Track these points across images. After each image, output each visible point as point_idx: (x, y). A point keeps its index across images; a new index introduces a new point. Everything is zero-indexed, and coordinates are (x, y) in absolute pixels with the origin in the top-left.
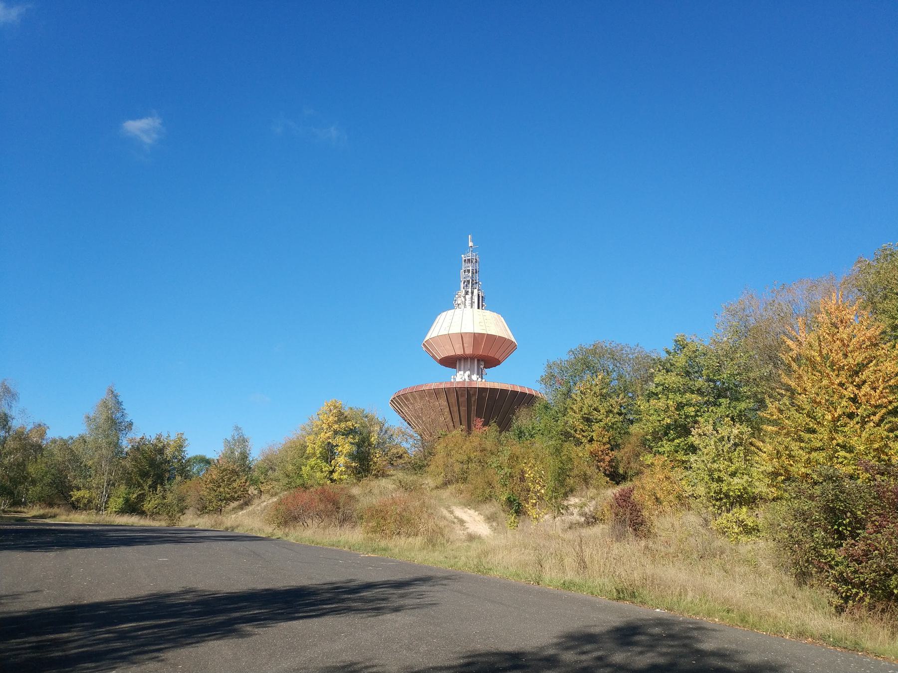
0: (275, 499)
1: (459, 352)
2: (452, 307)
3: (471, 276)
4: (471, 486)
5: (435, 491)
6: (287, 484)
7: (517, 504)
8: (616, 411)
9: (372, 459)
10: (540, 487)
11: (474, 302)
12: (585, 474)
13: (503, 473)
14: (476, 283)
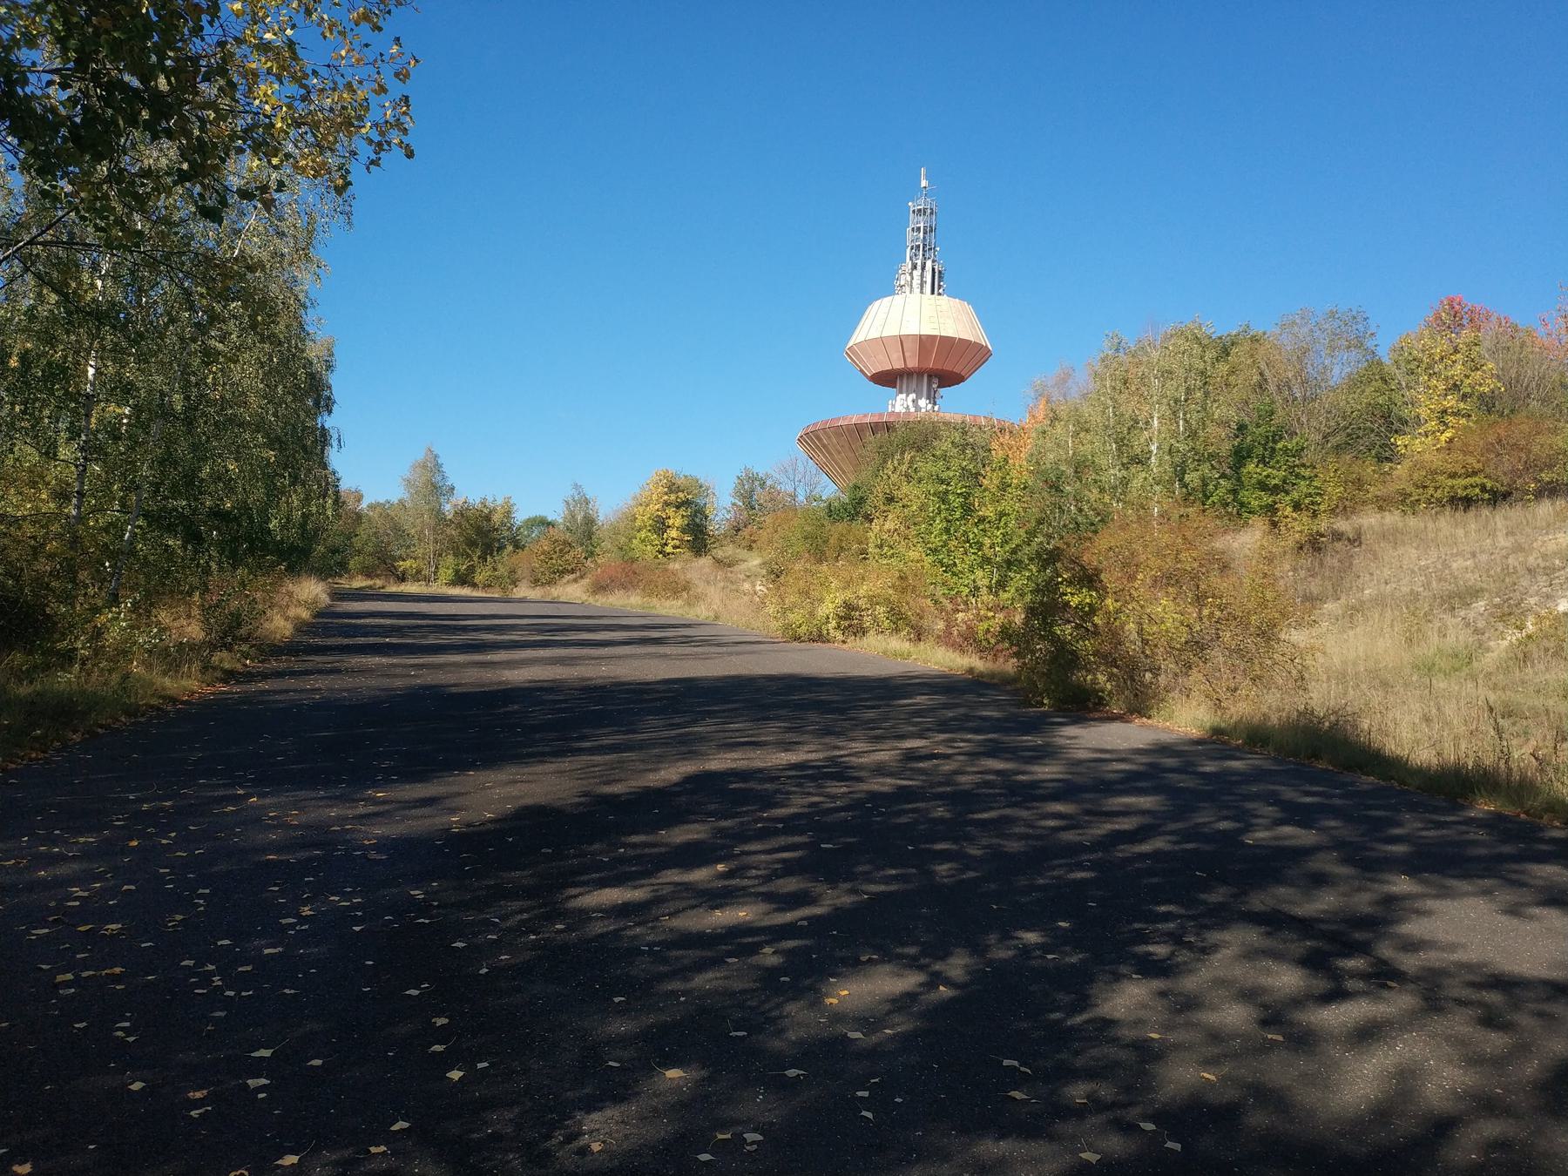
2: (892, 293)
11: (926, 282)
14: (930, 249)
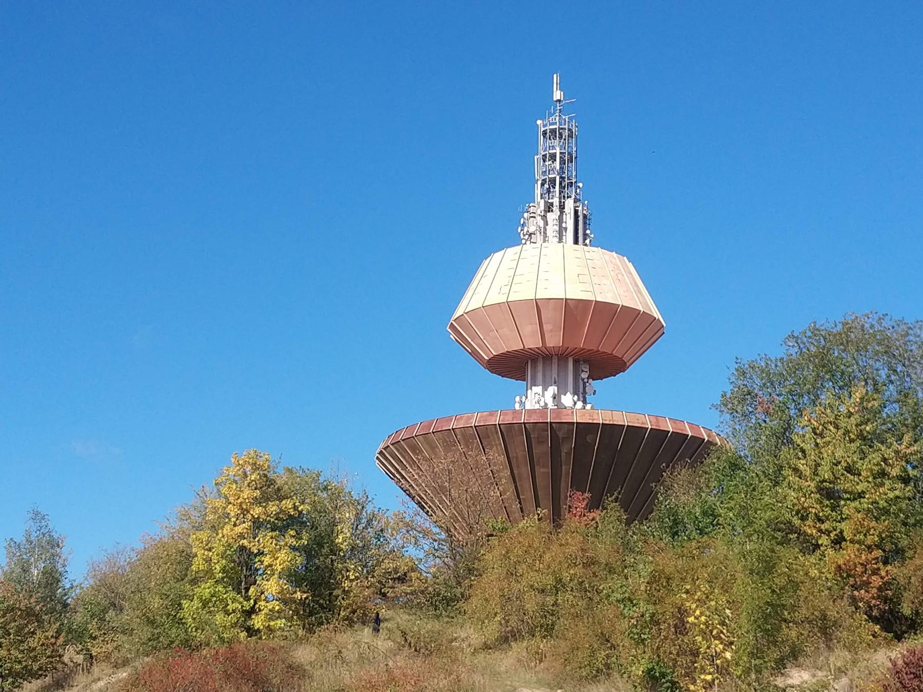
0: (123, 674)
1: (533, 342)
2: (517, 242)
3: (558, 168)
4: (563, 644)
5: (481, 656)
6: (150, 640)
7: (668, 684)
8: (895, 472)
9: (338, 584)
10: (721, 646)
11: (566, 229)
12: (824, 617)
13: (636, 615)
14: (571, 184)
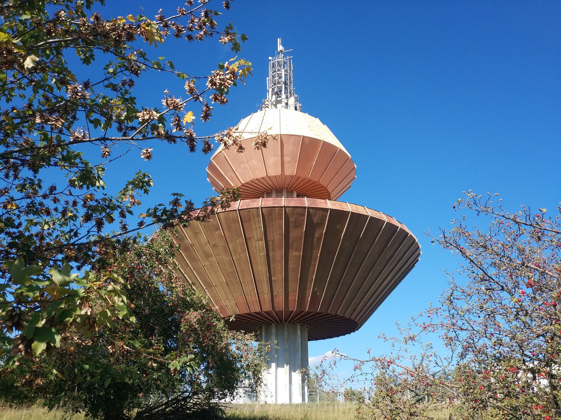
1: (274, 171)
